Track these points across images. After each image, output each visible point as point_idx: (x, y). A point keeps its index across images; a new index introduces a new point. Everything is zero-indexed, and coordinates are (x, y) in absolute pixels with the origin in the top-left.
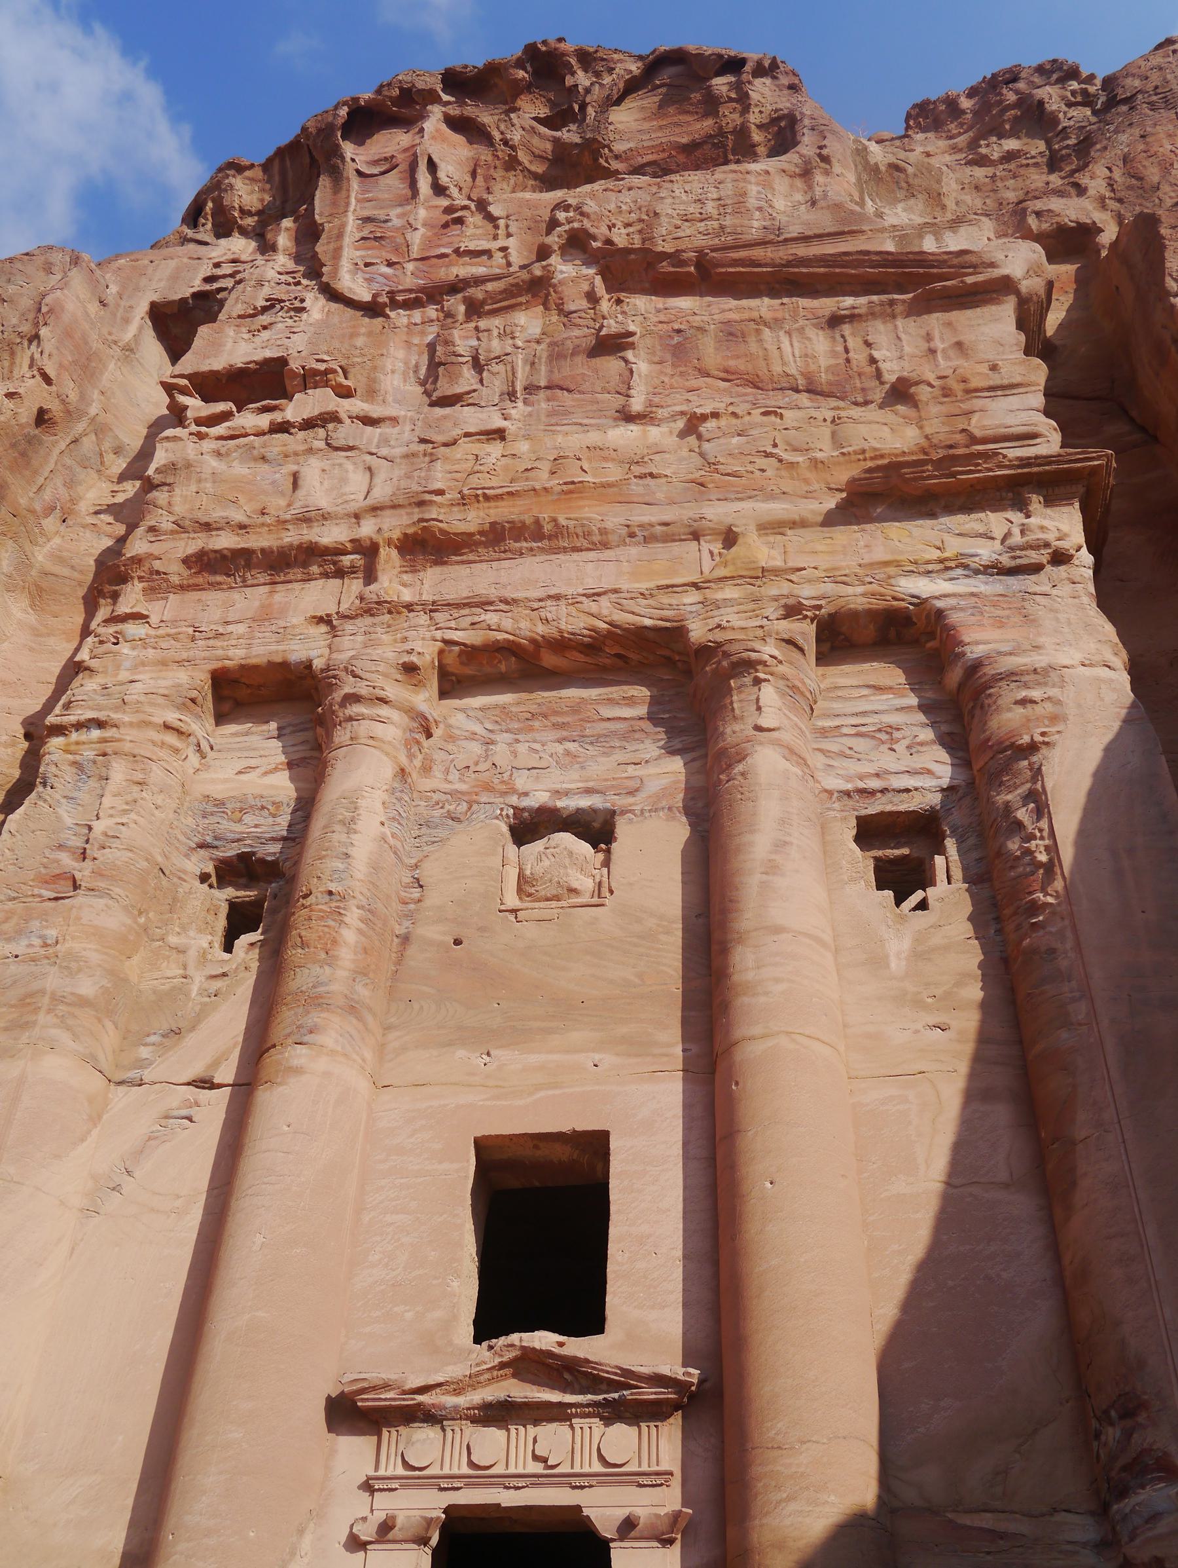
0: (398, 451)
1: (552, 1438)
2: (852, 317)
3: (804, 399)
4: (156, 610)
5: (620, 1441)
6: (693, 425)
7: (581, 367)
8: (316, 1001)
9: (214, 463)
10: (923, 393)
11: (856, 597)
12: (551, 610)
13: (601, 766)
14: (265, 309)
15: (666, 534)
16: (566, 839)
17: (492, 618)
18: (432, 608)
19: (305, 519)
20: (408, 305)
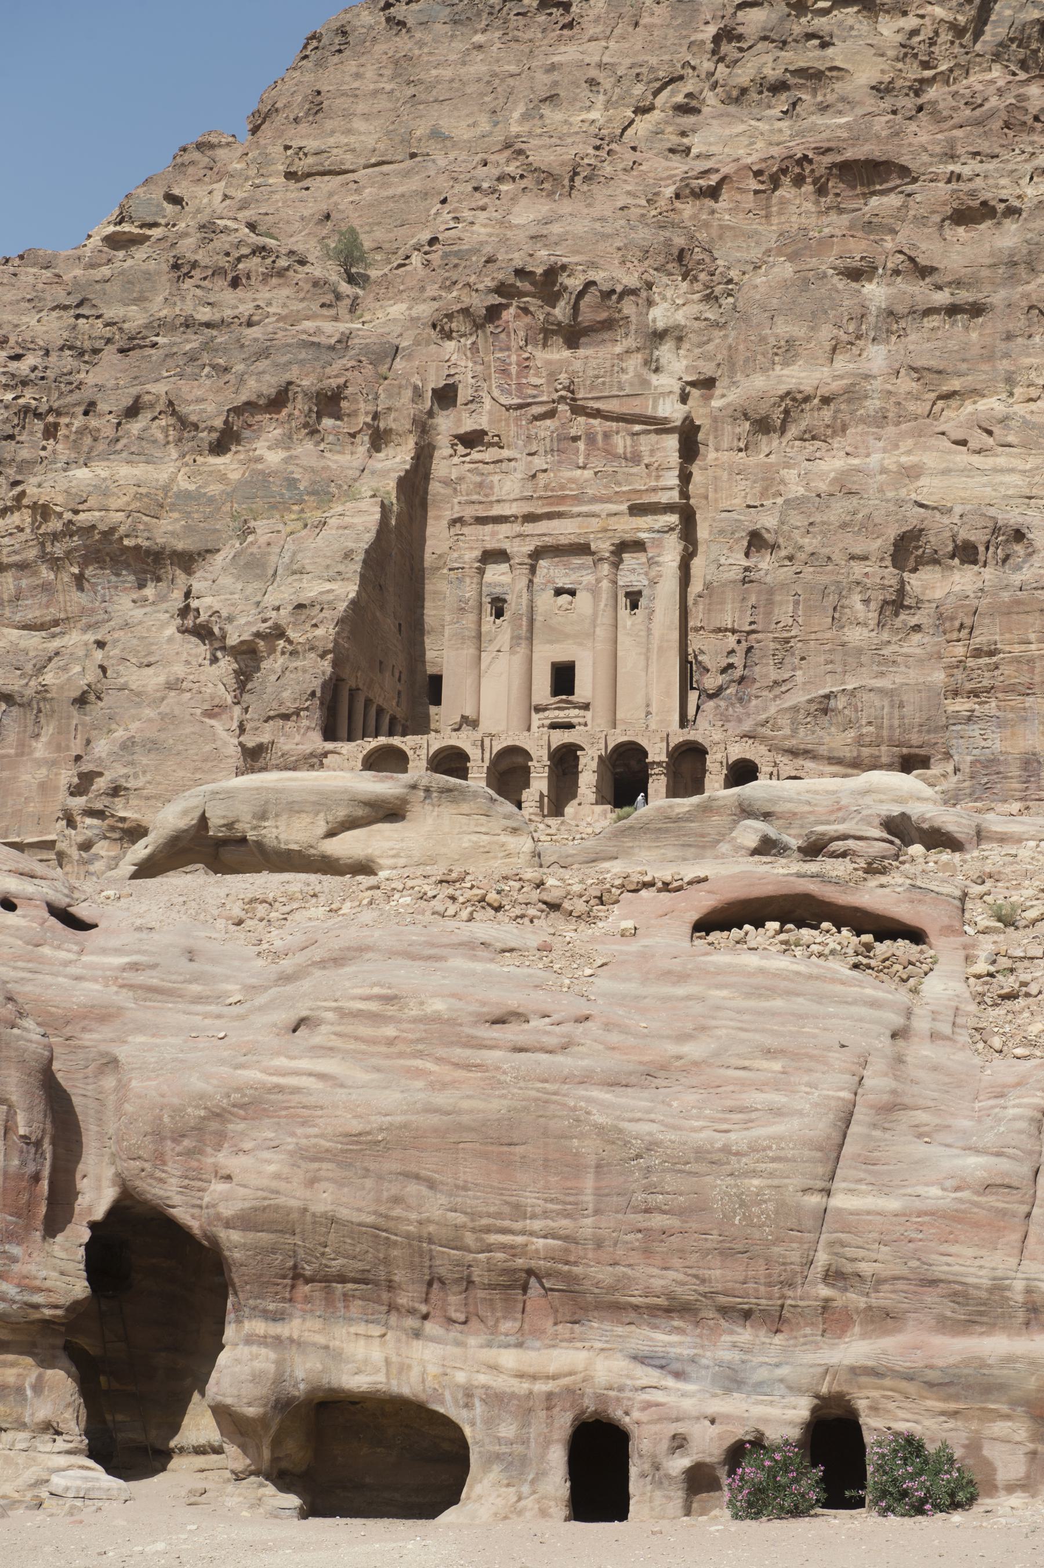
0: (520, 476)
1: (567, 712)
2: (637, 434)
3: (624, 464)
4: (466, 530)
5: (577, 712)
6: (596, 473)
7: (564, 445)
8: (520, 638)
9: (469, 475)
10: (652, 468)
11: (628, 537)
12: (561, 537)
13: (574, 577)
14: (472, 401)
15: (588, 515)
16: (565, 596)
17: (546, 539)
18: (532, 535)
19: (498, 501)
20: (516, 409)
